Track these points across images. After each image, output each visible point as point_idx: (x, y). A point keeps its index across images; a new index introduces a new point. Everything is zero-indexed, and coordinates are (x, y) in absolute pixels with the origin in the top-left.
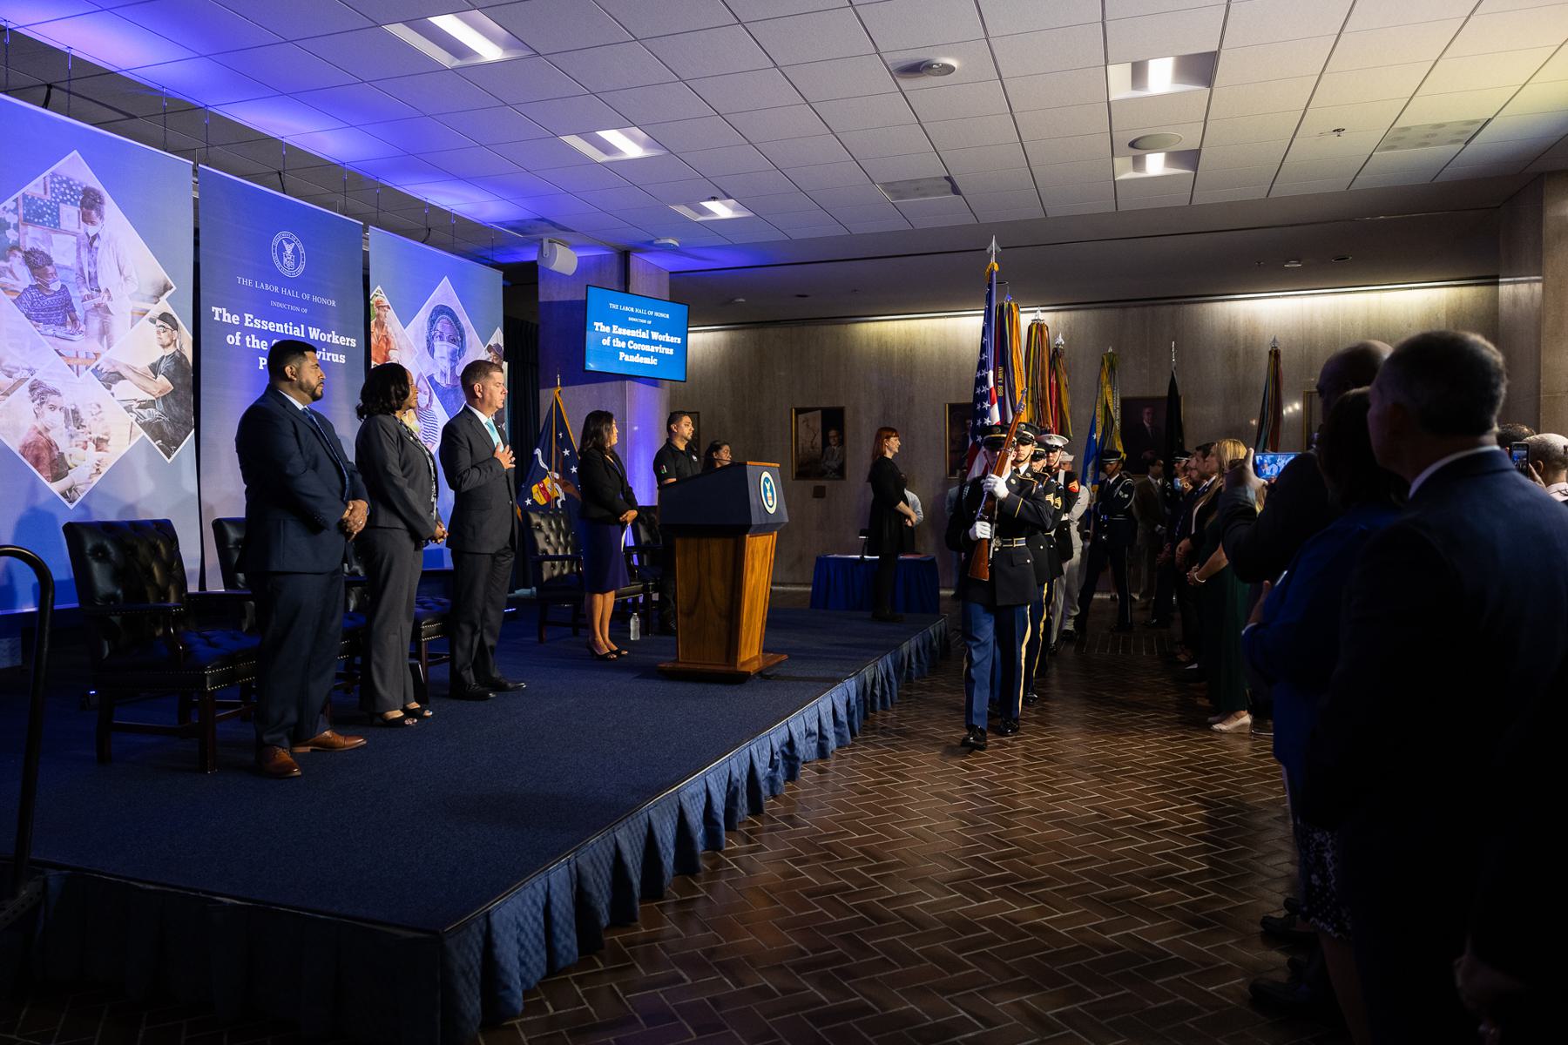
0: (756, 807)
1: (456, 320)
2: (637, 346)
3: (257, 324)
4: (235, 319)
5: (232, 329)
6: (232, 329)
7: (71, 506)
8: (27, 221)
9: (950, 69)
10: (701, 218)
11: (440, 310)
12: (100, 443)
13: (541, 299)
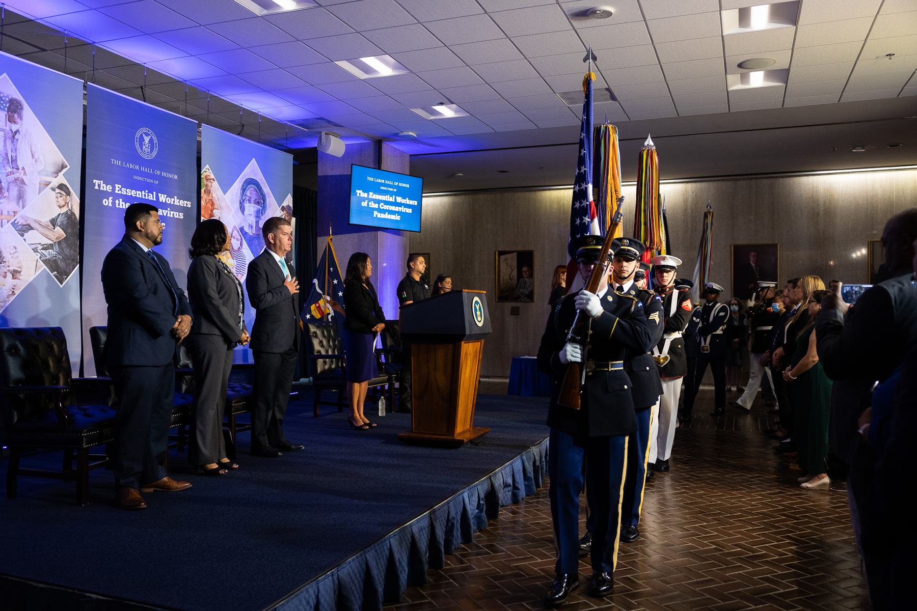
0: (467, 537)
1: (260, 189)
2: (386, 207)
5: (106, 195)
9: (609, 14)
10: (432, 118)
11: (250, 182)
12: (15, 274)
13: (320, 174)
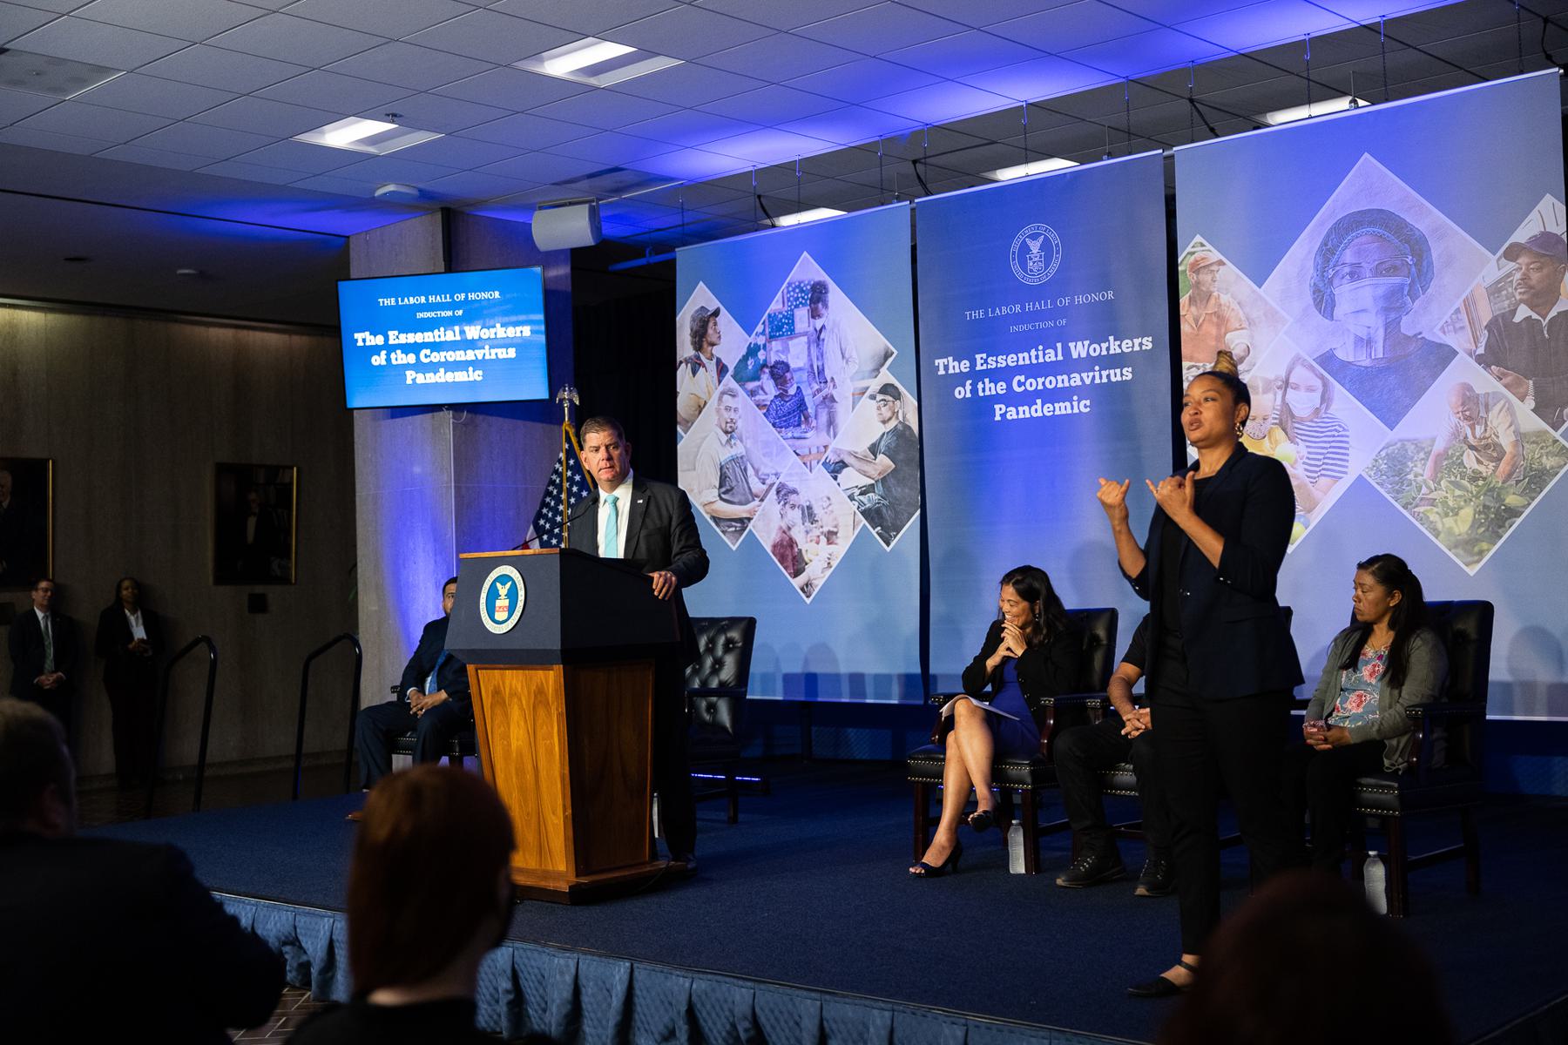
4: (965, 366)
5: (960, 379)
7: (808, 601)
8: (772, 338)
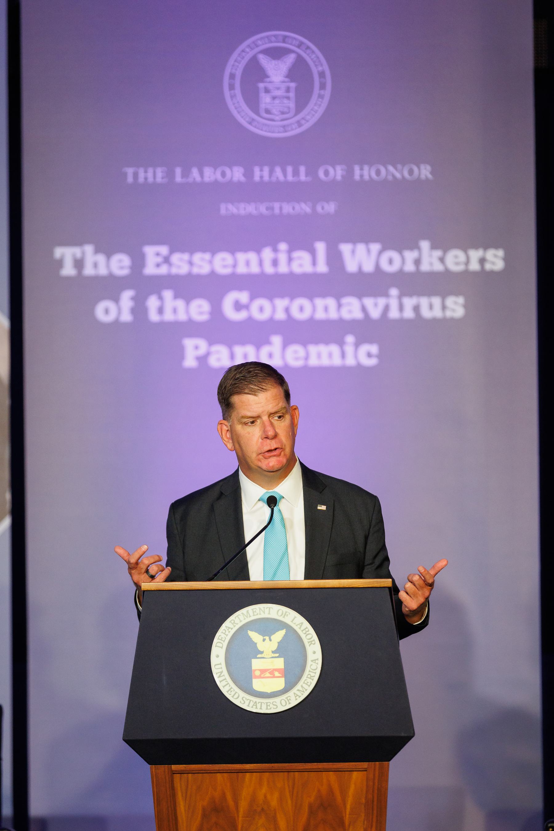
3: (180, 264)
5: (110, 287)
6: (110, 287)
